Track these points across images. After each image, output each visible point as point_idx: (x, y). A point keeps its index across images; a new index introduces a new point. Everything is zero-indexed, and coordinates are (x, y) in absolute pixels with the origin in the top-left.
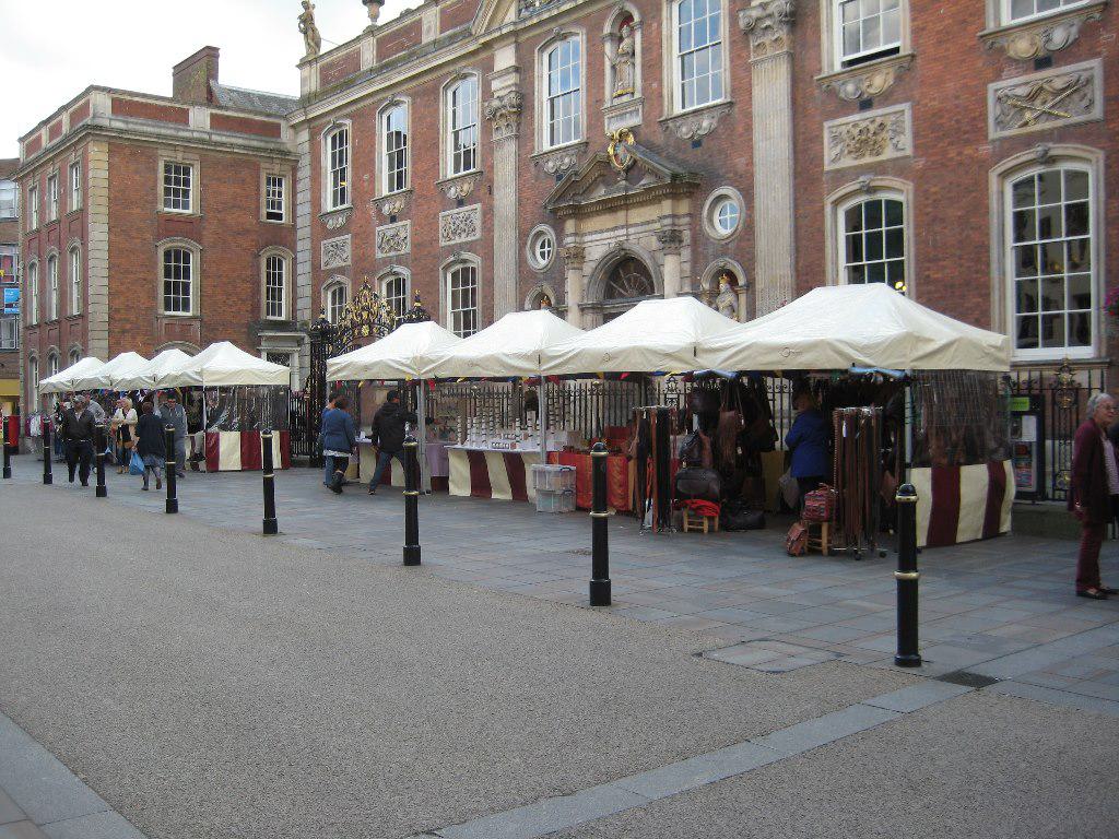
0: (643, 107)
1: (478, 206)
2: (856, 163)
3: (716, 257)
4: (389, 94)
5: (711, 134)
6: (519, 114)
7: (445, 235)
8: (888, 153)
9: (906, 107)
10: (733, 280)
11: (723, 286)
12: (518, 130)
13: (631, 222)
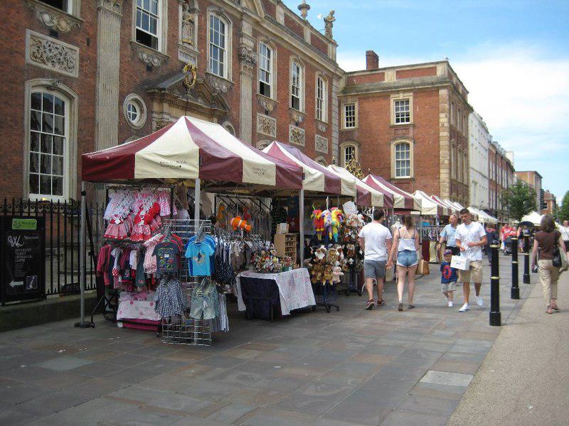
1: (77, 49)
9: (275, 120)
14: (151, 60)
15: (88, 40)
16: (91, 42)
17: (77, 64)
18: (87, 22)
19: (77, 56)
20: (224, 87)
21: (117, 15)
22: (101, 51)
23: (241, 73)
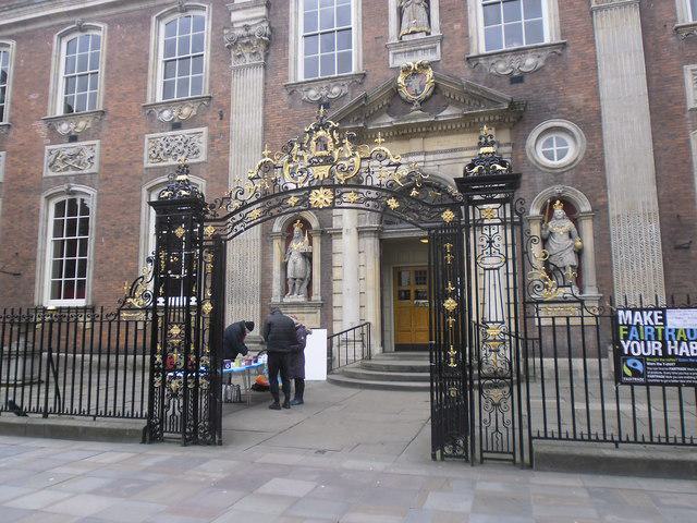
3: (548, 185)
4: (78, 19)
5: (537, 71)
6: (268, 45)
7: (154, 155)
10: (570, 209)
11: (559, 211)
13: (427, 150)
16: (223, 115)
21: (256, 65)
22: (233, 117)
23: (592, 13)
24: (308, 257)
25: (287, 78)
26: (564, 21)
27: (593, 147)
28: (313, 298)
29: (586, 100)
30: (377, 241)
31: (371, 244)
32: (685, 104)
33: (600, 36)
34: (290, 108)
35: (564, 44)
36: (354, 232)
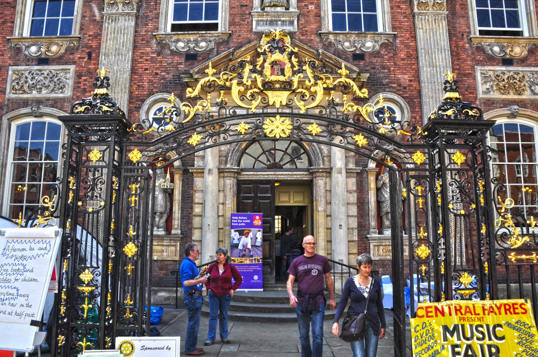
0: (298, 20)
2: (504, 97)
5: (375, 54)
8: (527, 95)
12: (138, 11)
14: (192, 46)
15: (89, 55)
17: (71, 82)
18: (90, 36)
19: (71, 75)
20: (369, 44)
22: (102, 58)
23: (414, 16)
24: (169, 194)
25: (157, 29)
26: (394, 18)
27: (415, 118)
28: (173, 232)
29: (410, 81)
30: (235, 181)
31: (230, 182)
32: (476, 94)
33: (420, 34)
34: (159, 55)
35: (395, 35)
36: (216, 171)
